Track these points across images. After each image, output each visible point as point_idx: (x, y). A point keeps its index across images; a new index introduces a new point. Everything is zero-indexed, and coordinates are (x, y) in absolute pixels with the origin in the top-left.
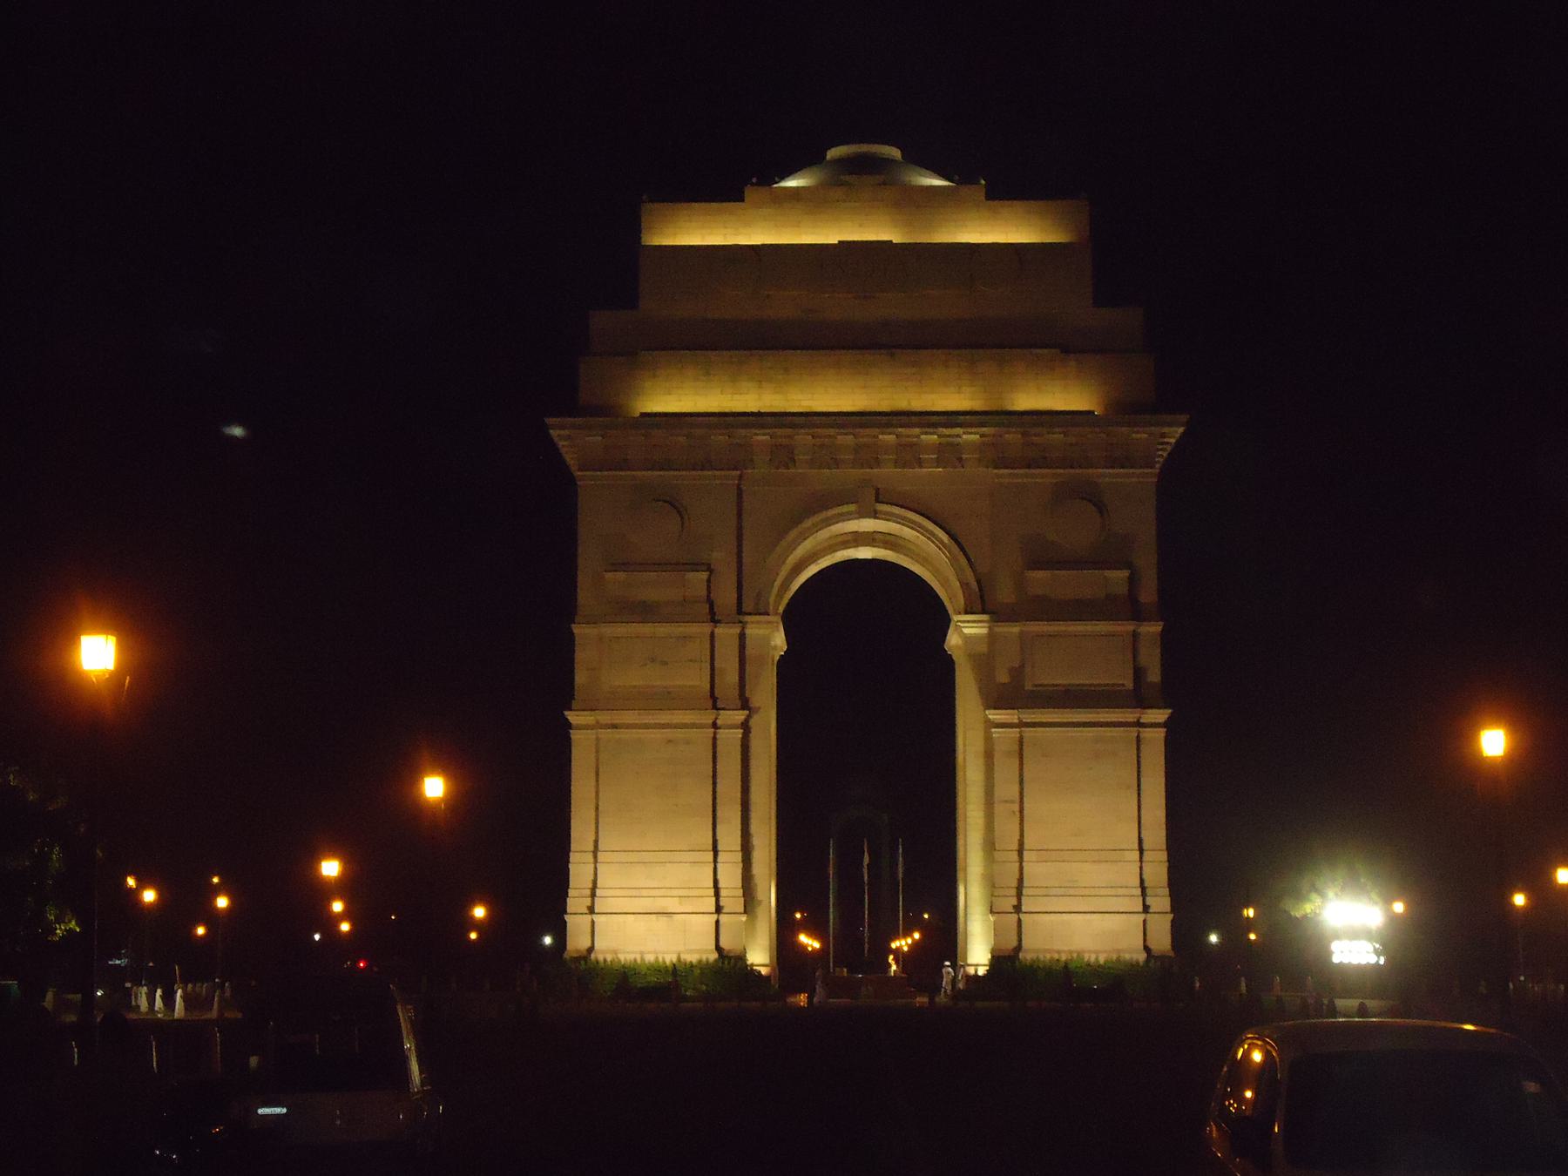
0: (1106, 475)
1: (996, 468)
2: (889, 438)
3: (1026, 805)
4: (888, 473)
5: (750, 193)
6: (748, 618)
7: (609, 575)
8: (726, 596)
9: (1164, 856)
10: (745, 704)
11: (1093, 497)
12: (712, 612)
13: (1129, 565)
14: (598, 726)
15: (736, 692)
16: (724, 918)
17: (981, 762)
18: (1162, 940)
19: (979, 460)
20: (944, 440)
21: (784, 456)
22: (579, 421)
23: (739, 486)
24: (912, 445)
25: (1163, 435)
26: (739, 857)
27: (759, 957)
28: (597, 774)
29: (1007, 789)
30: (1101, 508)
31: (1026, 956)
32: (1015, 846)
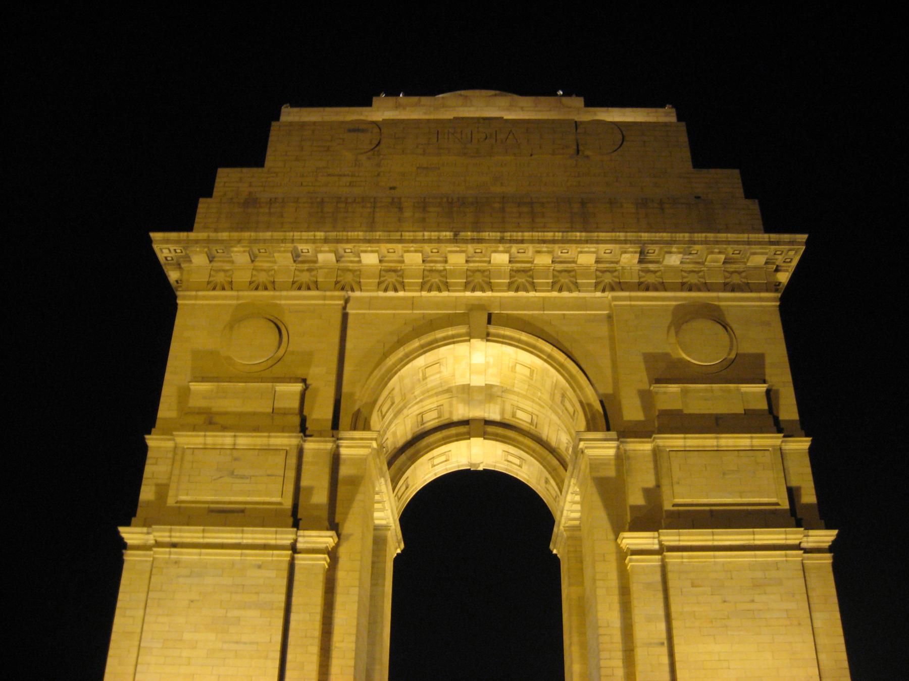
0: (725, 299)
1: (613, 289)
3: (677, 649)
6: (342, 434)
7: (195, 387)
8: (321, 412)
11: (716, 315)
13: (764, 382)
14: (158, 544)
15: (324, 514)
17: (615, 599)
19: (596, 285)
20: (559, 267)
22: (183, 235)
23: (345, 308)
24: (525, 271)
25: (777, 270)
29: (647, 629)
30: (725, 326)
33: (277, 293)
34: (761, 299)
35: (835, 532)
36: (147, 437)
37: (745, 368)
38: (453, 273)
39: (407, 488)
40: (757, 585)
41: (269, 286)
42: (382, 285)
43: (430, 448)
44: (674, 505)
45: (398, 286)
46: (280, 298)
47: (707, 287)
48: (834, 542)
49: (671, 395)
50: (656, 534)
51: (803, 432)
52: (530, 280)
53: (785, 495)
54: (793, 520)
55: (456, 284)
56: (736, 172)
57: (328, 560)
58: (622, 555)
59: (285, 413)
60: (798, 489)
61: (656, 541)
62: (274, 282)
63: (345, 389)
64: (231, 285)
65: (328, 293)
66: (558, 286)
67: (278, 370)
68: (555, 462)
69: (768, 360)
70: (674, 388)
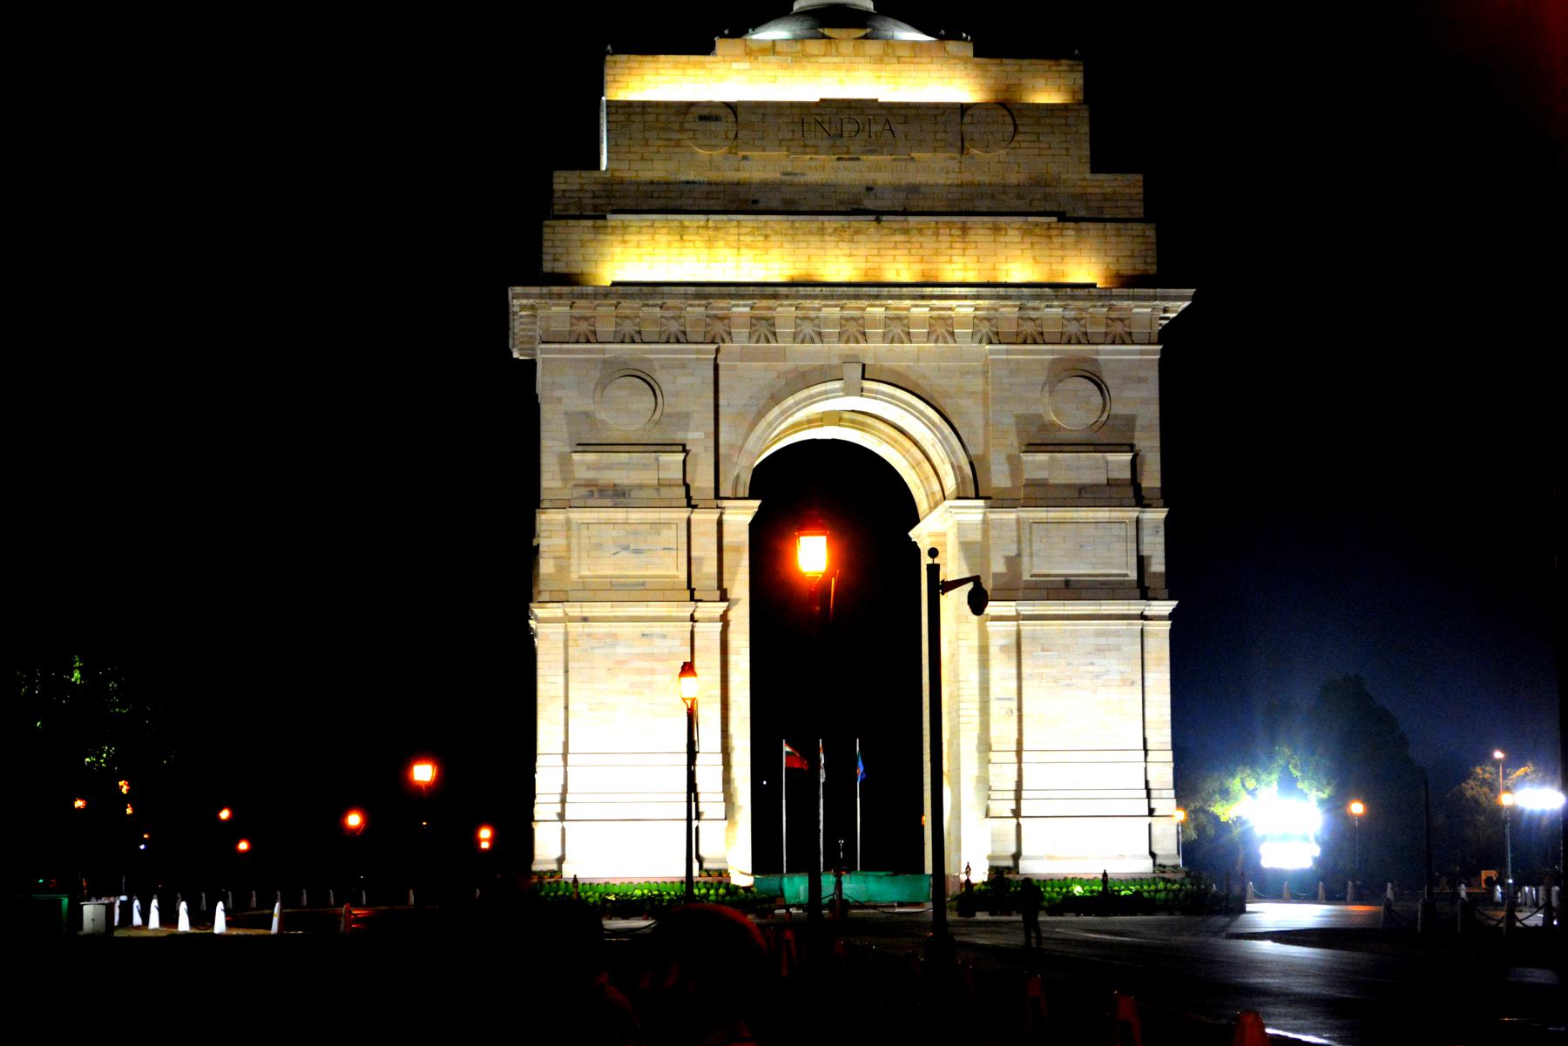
2: (876, 311)
4: (874, 349)
5: (721, 45)
6: (725, 503)
7: (576, 457)
8: (703, 480)
9: (1169, 756)
10: (724, 597)
12: (688, 497)
13: (1131, 447)
15: (715, 584)
18: (1168, 847)
20: (934, 313)
21: (765, 329)
22: (545, 290)
25: (1165, 310)
26: (719, 758)
28: (566, 672)
31: (1029, 867)
32: (1014, 747)
34: (1142, 353)
35: (1175, 603)
38: (826, 321)
40: (1100, 650)
41: (637, 338)
47: (1085, 338)
49: (1038, 464)
51: (1161, 502)
56: (1139, 177)
62: (639, 332)
63: (722, 450)
67: (657, 437)
68: (920, 456)
69: (1138, 423)
70: (1042, 457)
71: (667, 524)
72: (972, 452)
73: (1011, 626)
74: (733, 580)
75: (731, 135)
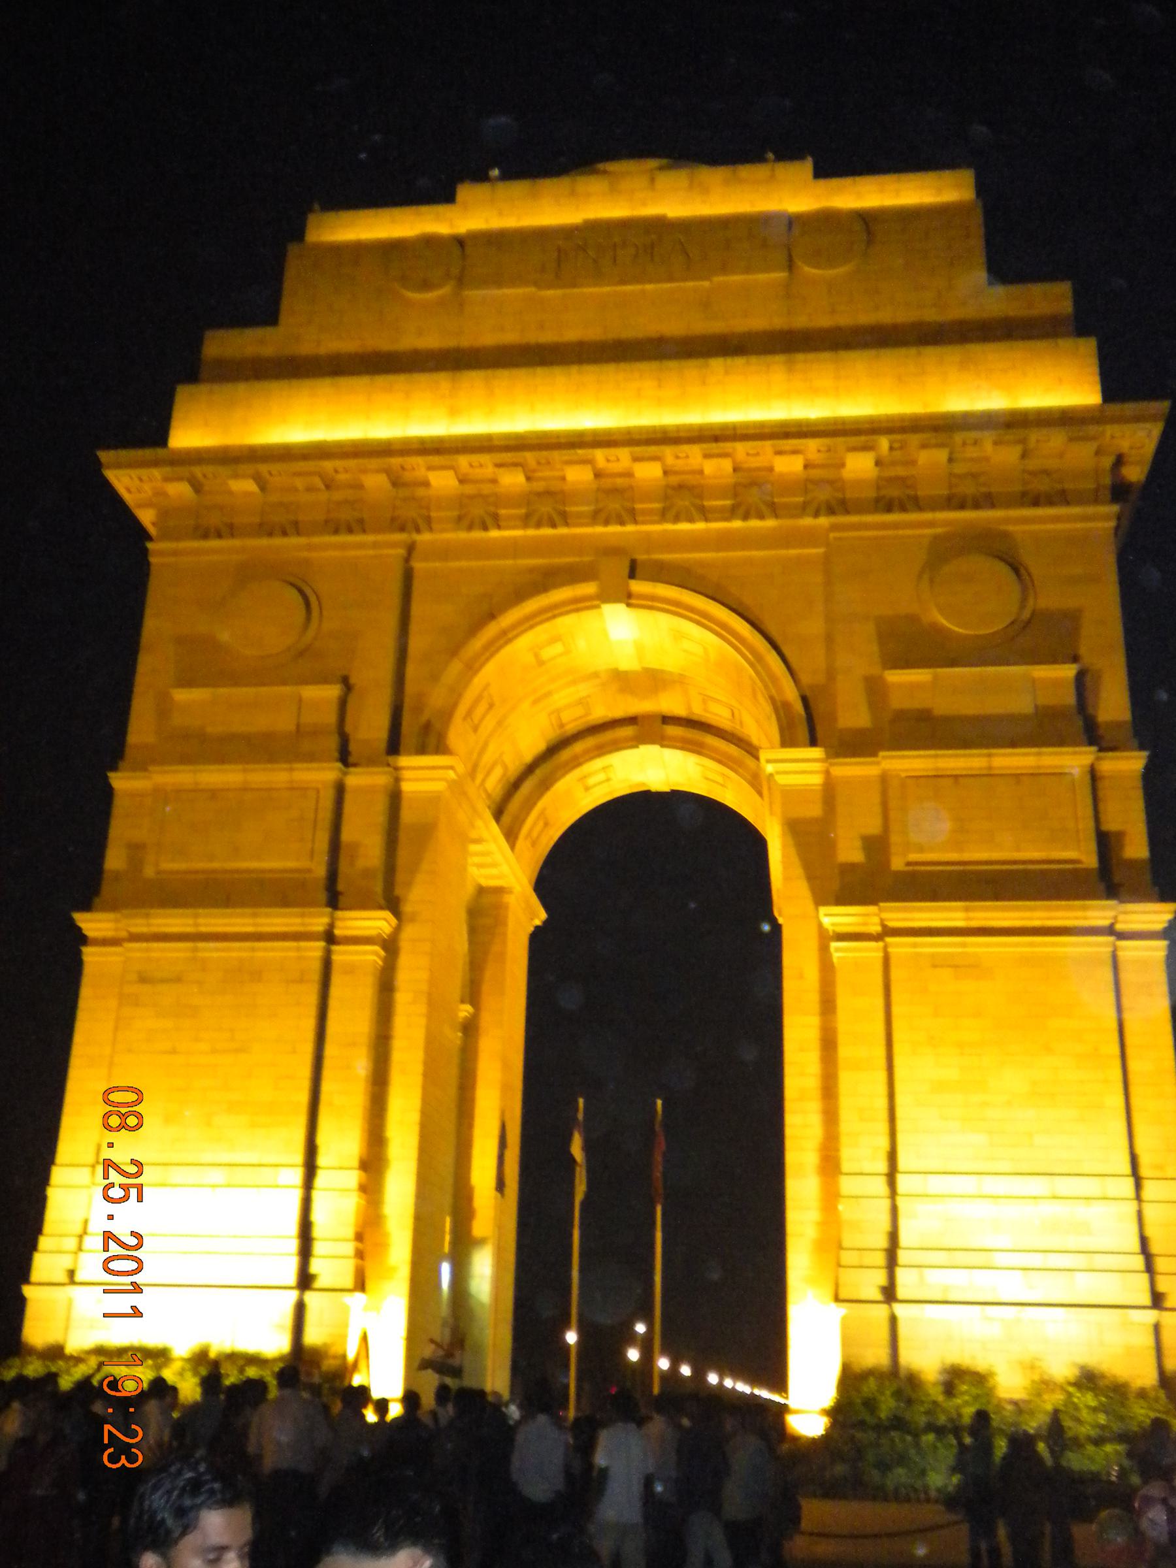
1: (831, 511)
5: (464, 192)
6: (404, 761)
7: (181, 696)
8: (371, 725)
13: (1075, 659)
16: (310, 1297)
23: (407, 560)
26: (353, 1178)
27: (386, 1378)
32: (882, 1166)
33: (302, 540)
34: (1085, 518)
36: (111, 775)
37: (1039, 635)
39: (546, 824)
42: (464, 521)
43: (576, 762)
44: (909, 864)
45: (489, 521)
46: (310, 547)
47: (987, 501)
48: (1170, 921)
50: (872, 909)
51: (1136, 743)
52: (698, 502)
53: (1093, 846)
54: (1102, 886)
55: (580, 515)
57: (382, 953)
58: (825, 938)
59: (316, 732)
60: (1120, 835)
61: (876, 920)
63: (410, 688)
64: (230, 530)
65: (380, 538)
66: (741, 511)
71: (301, 790)
72: (805, 679)
73: (871, 951)
74: (409, 884)
75: (455, 271)
